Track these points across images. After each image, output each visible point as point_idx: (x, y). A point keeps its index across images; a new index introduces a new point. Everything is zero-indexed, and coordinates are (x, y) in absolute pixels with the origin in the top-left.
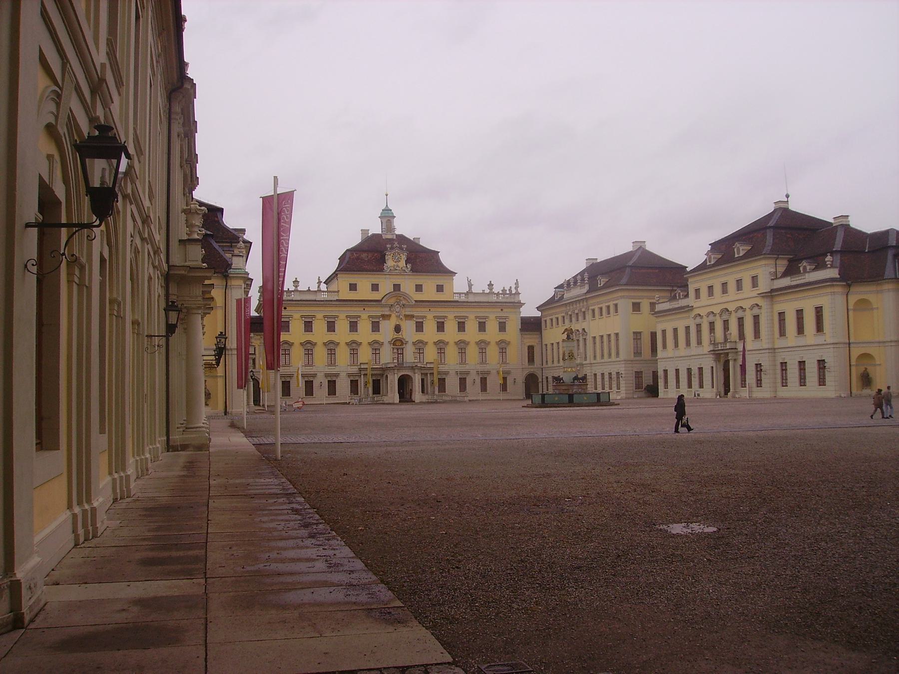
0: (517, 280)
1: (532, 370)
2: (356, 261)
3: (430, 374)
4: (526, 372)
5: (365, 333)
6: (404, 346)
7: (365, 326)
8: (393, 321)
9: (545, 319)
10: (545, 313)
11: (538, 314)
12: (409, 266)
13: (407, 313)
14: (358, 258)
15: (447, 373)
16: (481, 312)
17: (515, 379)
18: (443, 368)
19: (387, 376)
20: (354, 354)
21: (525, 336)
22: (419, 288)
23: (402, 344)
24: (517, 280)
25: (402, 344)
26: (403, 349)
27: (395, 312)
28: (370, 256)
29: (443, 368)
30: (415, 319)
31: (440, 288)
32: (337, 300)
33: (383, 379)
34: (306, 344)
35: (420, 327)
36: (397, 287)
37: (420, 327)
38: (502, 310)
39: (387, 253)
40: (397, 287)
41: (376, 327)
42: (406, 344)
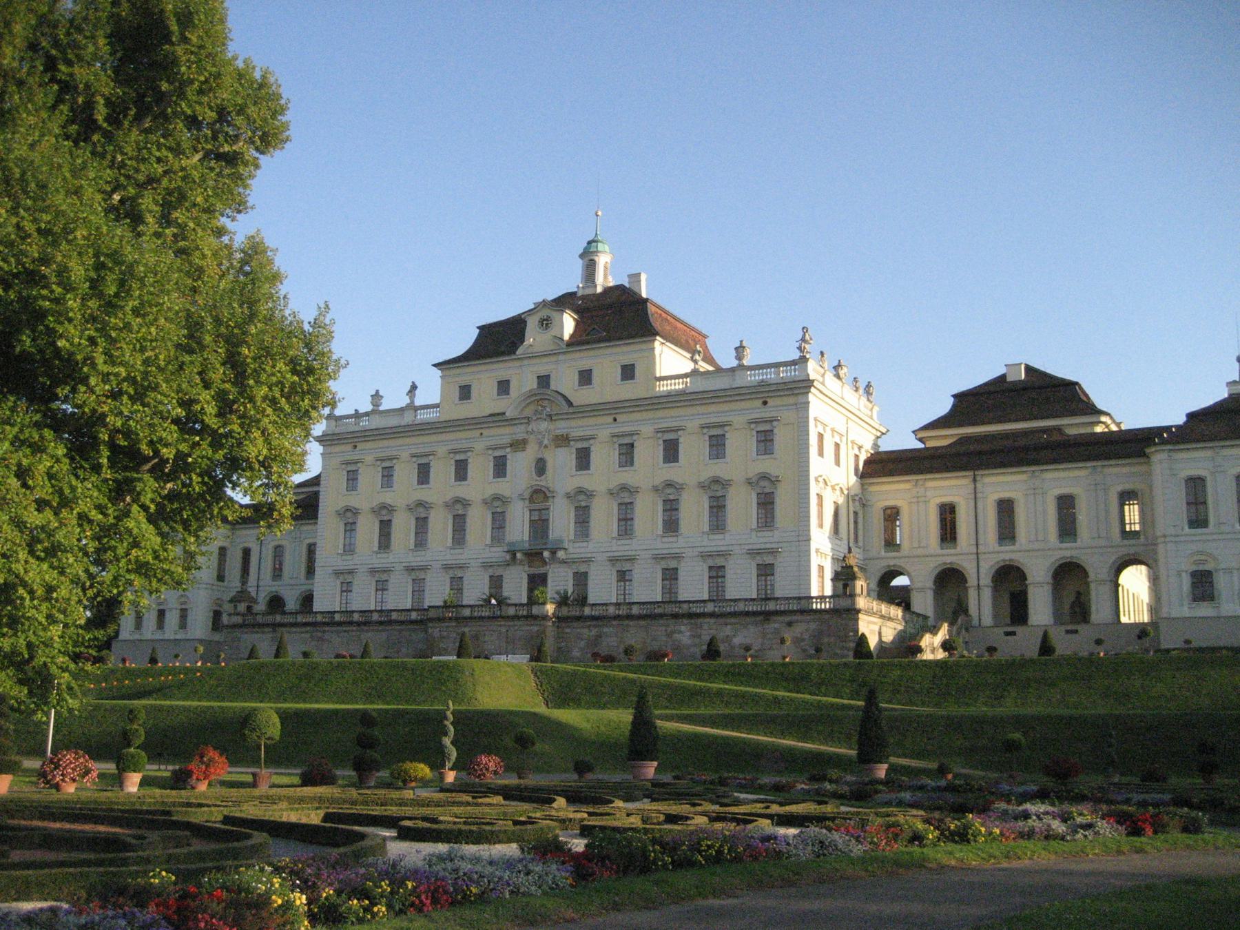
0: (805, 330)
5: (480, 485)
7: (480, 468)
13: (559, 432)
16: (714, 413)
18: (675, 545)
22: (586, 377)
23: (546, 498)
24: (805, 330)
25: (546, 498)
31: (628, 372)
35: (583, 458)
36: (544, 381)
38: (765, 403)
40: (544, 381)
41: (500, 468)
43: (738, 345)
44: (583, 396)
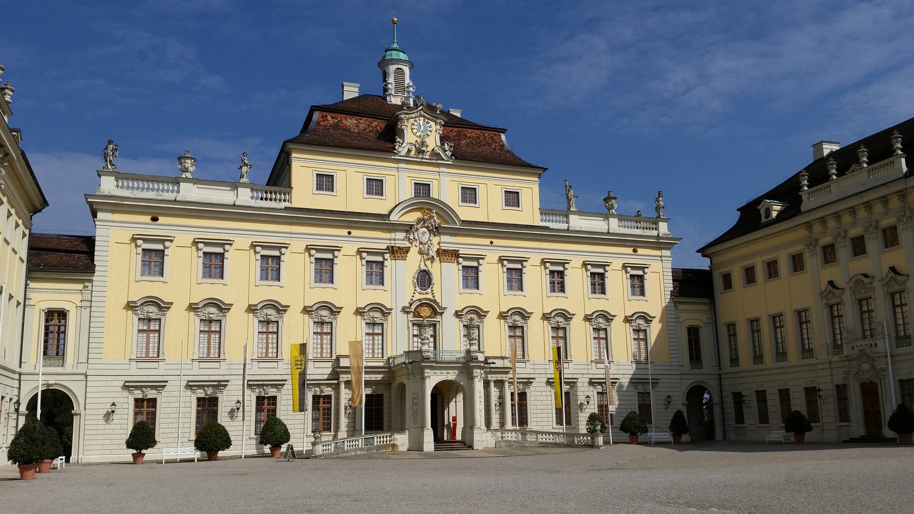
1: (699, 378)
2: (331, 131)
3: (496, 382)
4: (687, 384)
6: (438, 318)
8: (414, 262)
9: (725, 270)
10: (718, 260)
11: (703, 264)
12: (446, 147)
13: (444, 247)
14: (336, 126)
15: (528, 382)
17: (669, 397)
19: (402, 387)
20: (321, 334)
21: (681, 307)
22: (469, 195)
23: (435, 313)
25: (435, 313)
26: (434, 325)
27: (417, 244)
28: (362, 126)
29: (523, 371)
30: (461, 260)
32: (286, 208)
33: (390, 393)
34: (204, 306)
35: (472, 277)
36: (422, 189)
37: (472, 277)
38: (635, 251)
39: (403, 116)
40: (422, 189)
42: (441, 314)
43: (606, 196)
44: (466, 213)
